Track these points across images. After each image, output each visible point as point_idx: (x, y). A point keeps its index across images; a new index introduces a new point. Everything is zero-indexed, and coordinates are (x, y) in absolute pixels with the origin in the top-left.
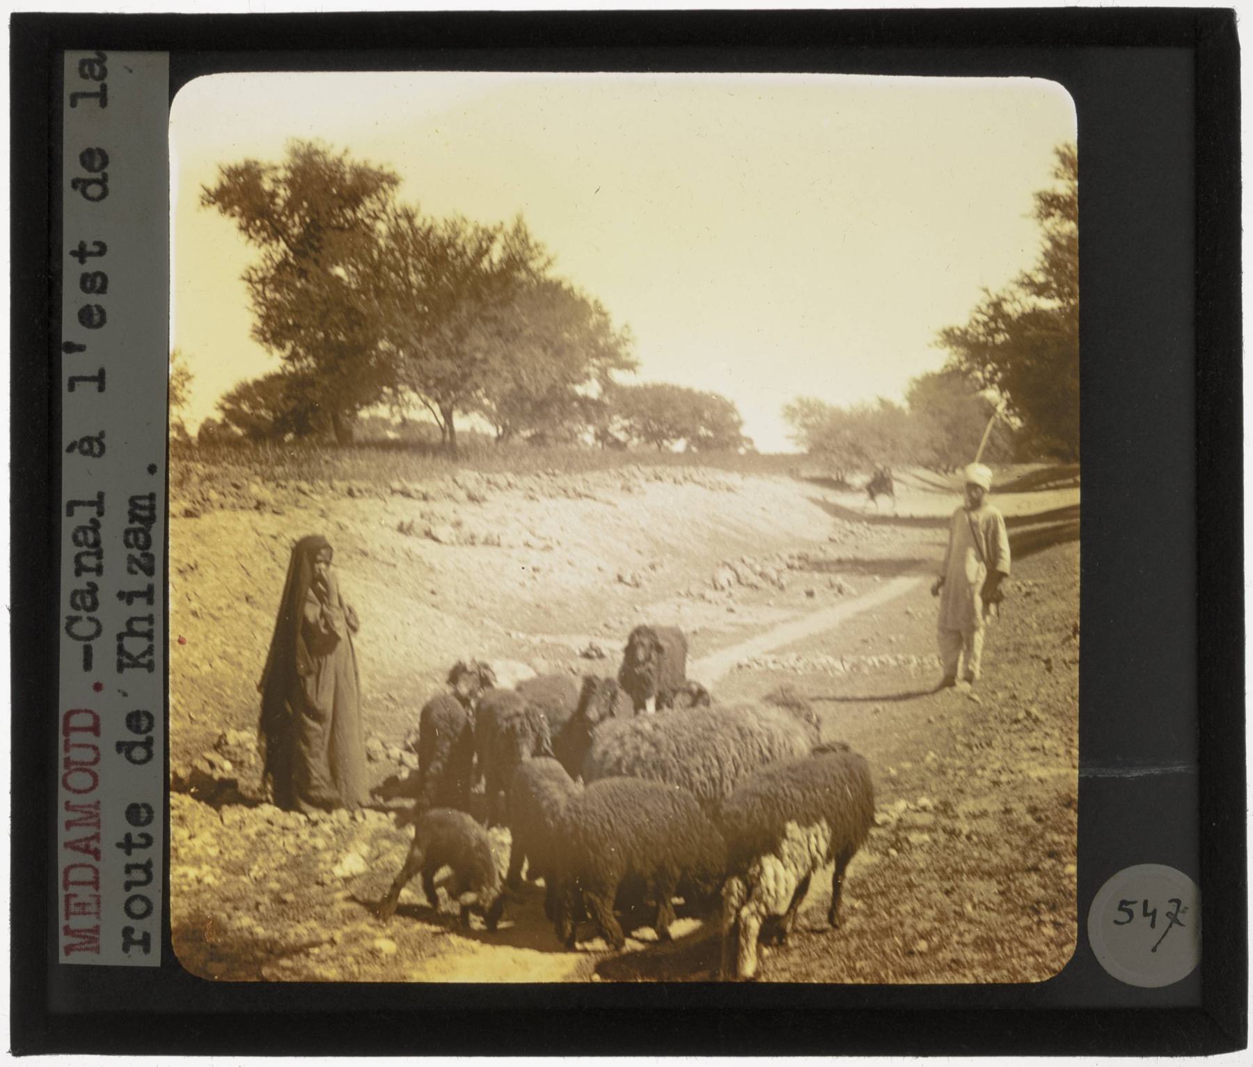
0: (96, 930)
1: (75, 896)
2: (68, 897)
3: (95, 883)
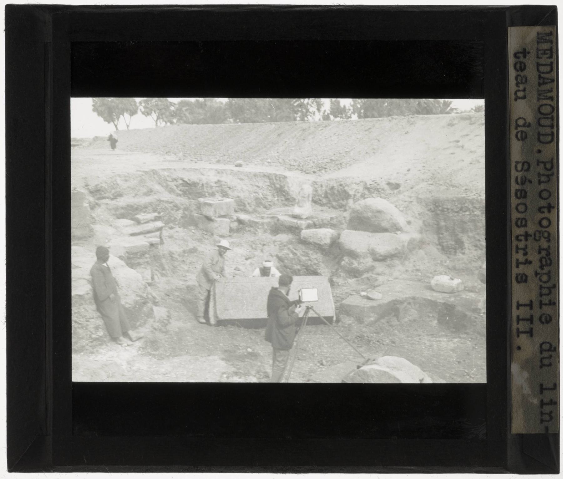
1: (548, 58)
3: (538, 65)
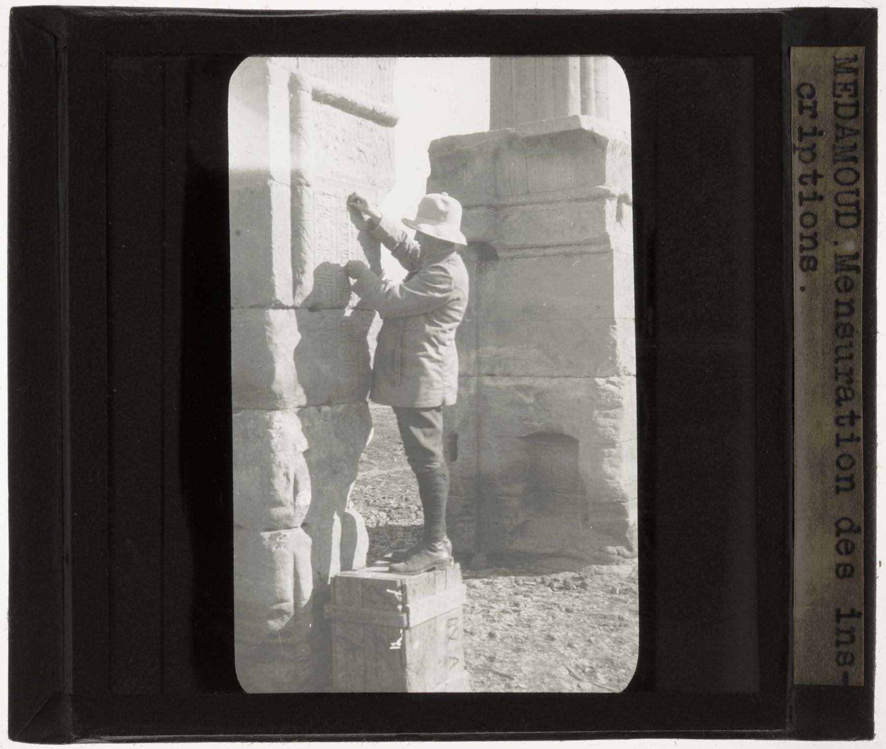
2: (855, 94)
3: (836, 106)
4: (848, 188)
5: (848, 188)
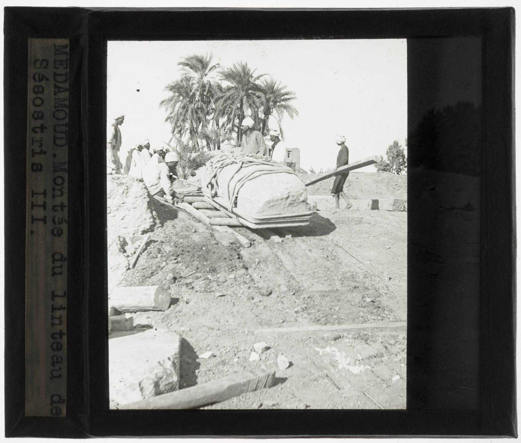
0: (56, 54)
1: (64, 68)
2: (66, 68)
3: (55, 75)
4: (62, 122)
5: (62, 122)
